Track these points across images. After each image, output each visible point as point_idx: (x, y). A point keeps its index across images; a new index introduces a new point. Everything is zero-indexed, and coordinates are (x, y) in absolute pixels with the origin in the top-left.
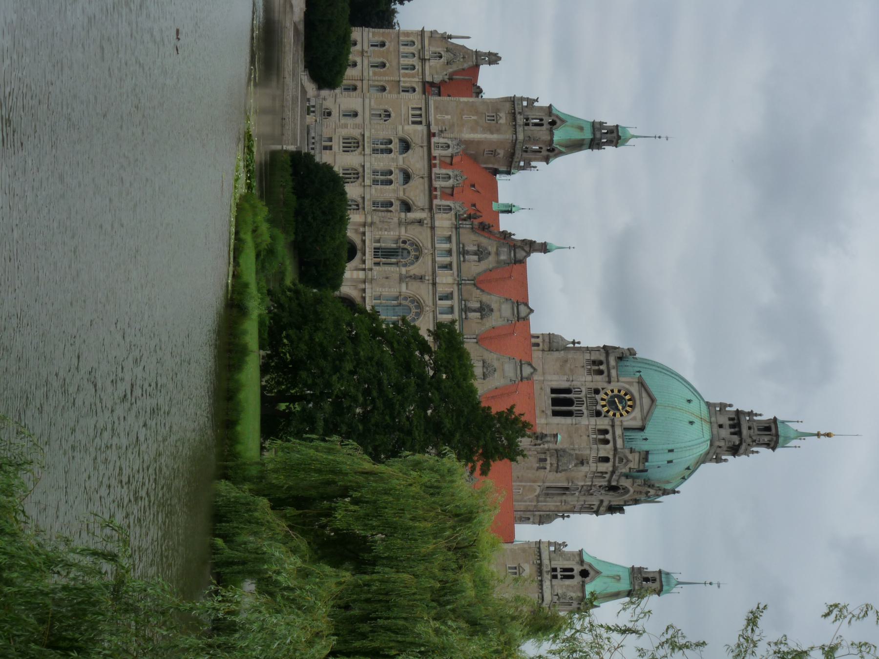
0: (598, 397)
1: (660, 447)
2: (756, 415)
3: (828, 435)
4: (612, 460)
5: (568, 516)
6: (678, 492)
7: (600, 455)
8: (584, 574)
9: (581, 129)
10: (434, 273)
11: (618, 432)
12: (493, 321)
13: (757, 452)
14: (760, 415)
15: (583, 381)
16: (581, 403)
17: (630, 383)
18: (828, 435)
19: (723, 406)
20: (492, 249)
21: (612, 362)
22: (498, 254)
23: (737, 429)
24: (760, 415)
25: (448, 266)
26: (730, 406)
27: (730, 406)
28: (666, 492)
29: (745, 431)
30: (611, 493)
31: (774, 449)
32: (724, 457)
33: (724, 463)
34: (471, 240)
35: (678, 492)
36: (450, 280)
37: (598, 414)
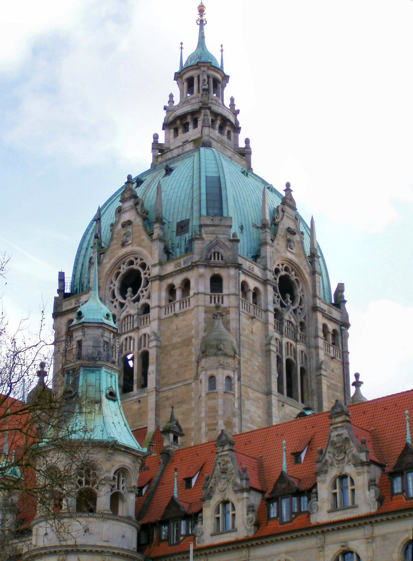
2: (171, 101)
3: (201, 10)
4: (217, 271)
5: (357, 376)
6: (288, 185)
7: (208, 291)
13: (232, 100)
14: (171, 96)
18: (201, 10)
19: (157, 147)
23: (189, 119)
24: (171, 96)
26: (156, 137)
27: (156, 137)
28: (288, 201)
30: (298, 292)
31: (226, 78)
32: (242, 144)
33: (251, 145)
35: (288, 185)
37: (146, 309)
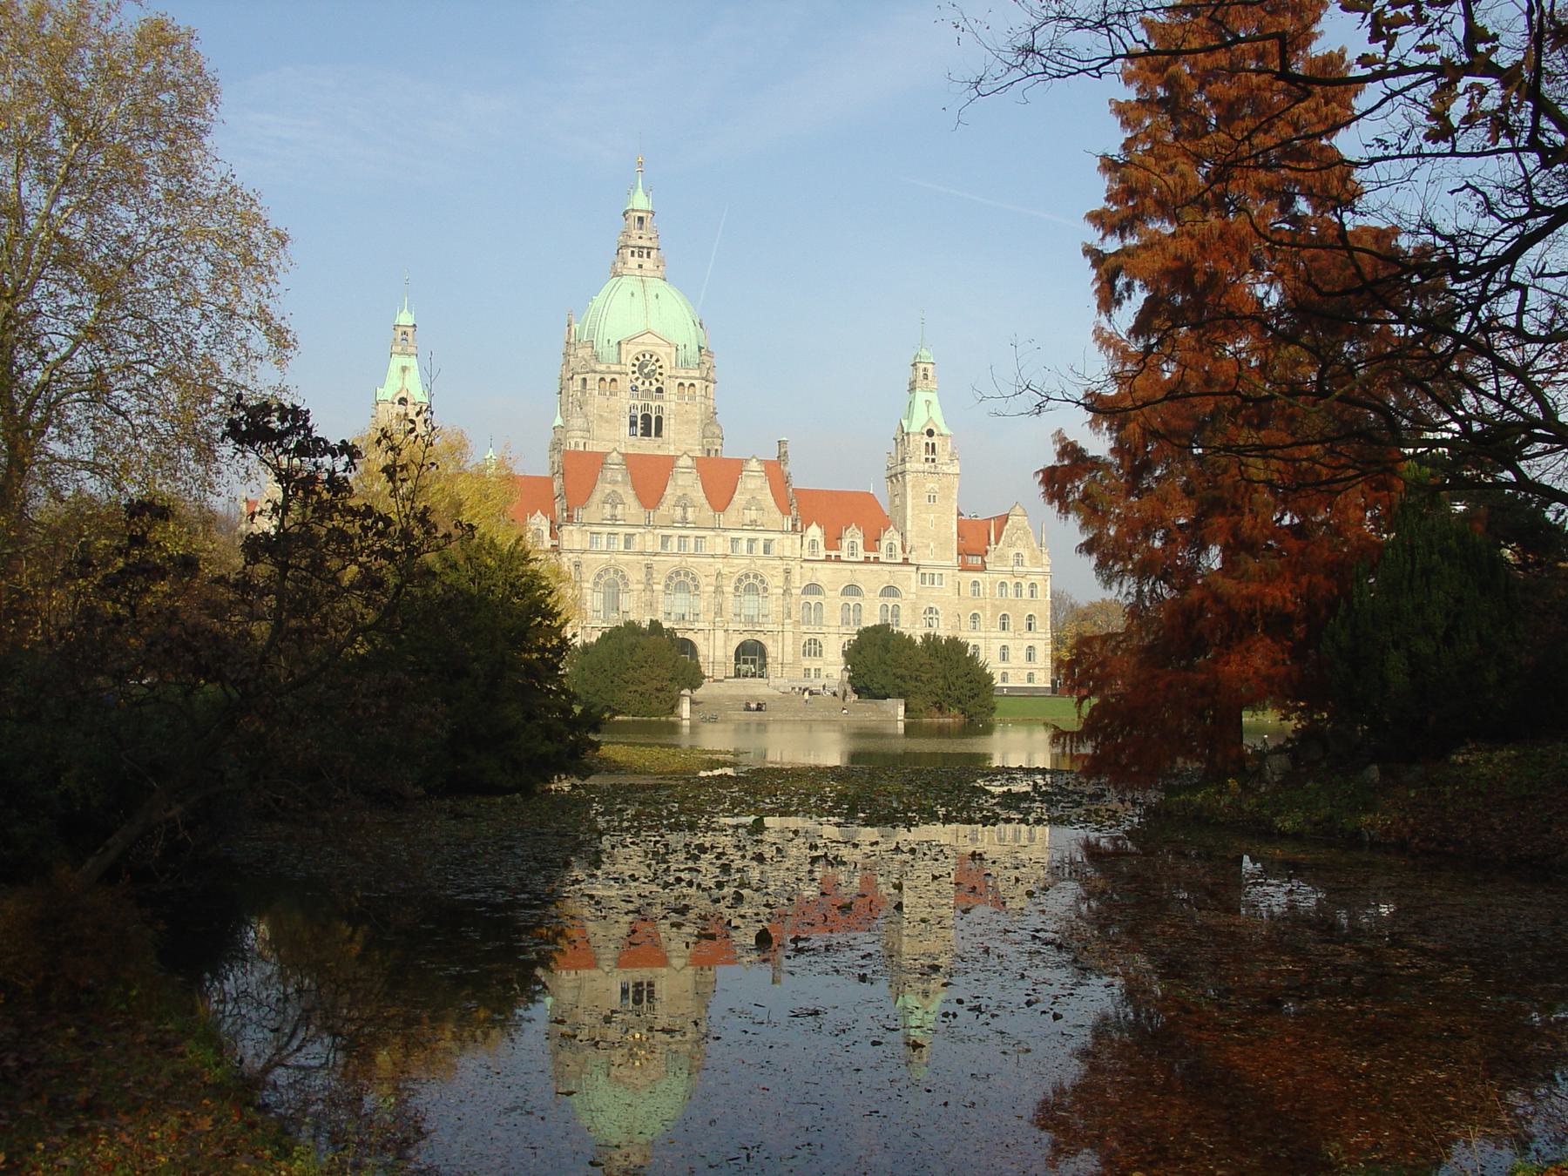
0: (641, 388)
1: (693, 334)
8: (930, 433)
9: (404, 369)
10: (642, 553)
11: (682, 373)
12: (698, 495)
15: (625, 402)
16: (646, 407)
17: (628, 352)
20: (608, 488)
21: (602, 367)
22: (616, 482)
25: (629, 539)
29: (649, 244)
34: (595, 510)
36: (649, 537)
37: (659, 390)
